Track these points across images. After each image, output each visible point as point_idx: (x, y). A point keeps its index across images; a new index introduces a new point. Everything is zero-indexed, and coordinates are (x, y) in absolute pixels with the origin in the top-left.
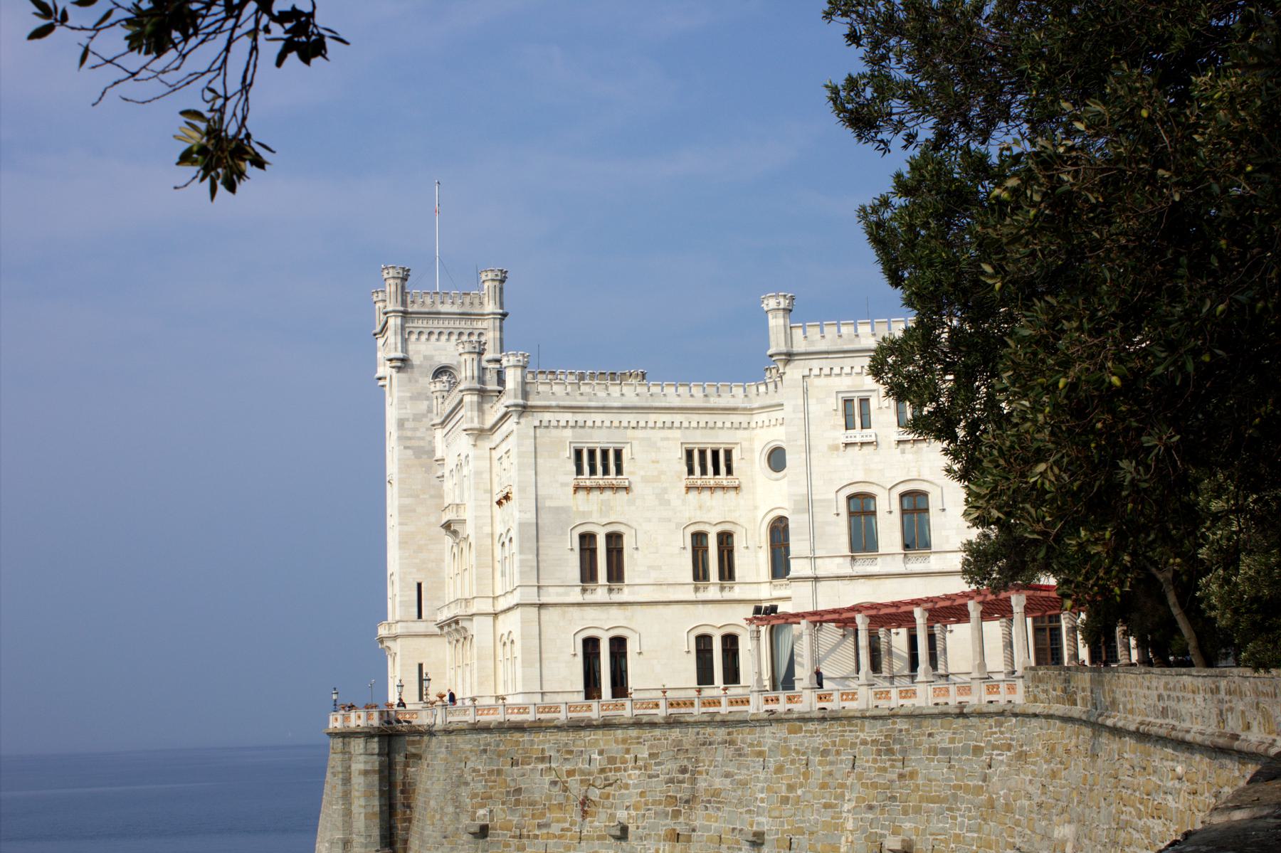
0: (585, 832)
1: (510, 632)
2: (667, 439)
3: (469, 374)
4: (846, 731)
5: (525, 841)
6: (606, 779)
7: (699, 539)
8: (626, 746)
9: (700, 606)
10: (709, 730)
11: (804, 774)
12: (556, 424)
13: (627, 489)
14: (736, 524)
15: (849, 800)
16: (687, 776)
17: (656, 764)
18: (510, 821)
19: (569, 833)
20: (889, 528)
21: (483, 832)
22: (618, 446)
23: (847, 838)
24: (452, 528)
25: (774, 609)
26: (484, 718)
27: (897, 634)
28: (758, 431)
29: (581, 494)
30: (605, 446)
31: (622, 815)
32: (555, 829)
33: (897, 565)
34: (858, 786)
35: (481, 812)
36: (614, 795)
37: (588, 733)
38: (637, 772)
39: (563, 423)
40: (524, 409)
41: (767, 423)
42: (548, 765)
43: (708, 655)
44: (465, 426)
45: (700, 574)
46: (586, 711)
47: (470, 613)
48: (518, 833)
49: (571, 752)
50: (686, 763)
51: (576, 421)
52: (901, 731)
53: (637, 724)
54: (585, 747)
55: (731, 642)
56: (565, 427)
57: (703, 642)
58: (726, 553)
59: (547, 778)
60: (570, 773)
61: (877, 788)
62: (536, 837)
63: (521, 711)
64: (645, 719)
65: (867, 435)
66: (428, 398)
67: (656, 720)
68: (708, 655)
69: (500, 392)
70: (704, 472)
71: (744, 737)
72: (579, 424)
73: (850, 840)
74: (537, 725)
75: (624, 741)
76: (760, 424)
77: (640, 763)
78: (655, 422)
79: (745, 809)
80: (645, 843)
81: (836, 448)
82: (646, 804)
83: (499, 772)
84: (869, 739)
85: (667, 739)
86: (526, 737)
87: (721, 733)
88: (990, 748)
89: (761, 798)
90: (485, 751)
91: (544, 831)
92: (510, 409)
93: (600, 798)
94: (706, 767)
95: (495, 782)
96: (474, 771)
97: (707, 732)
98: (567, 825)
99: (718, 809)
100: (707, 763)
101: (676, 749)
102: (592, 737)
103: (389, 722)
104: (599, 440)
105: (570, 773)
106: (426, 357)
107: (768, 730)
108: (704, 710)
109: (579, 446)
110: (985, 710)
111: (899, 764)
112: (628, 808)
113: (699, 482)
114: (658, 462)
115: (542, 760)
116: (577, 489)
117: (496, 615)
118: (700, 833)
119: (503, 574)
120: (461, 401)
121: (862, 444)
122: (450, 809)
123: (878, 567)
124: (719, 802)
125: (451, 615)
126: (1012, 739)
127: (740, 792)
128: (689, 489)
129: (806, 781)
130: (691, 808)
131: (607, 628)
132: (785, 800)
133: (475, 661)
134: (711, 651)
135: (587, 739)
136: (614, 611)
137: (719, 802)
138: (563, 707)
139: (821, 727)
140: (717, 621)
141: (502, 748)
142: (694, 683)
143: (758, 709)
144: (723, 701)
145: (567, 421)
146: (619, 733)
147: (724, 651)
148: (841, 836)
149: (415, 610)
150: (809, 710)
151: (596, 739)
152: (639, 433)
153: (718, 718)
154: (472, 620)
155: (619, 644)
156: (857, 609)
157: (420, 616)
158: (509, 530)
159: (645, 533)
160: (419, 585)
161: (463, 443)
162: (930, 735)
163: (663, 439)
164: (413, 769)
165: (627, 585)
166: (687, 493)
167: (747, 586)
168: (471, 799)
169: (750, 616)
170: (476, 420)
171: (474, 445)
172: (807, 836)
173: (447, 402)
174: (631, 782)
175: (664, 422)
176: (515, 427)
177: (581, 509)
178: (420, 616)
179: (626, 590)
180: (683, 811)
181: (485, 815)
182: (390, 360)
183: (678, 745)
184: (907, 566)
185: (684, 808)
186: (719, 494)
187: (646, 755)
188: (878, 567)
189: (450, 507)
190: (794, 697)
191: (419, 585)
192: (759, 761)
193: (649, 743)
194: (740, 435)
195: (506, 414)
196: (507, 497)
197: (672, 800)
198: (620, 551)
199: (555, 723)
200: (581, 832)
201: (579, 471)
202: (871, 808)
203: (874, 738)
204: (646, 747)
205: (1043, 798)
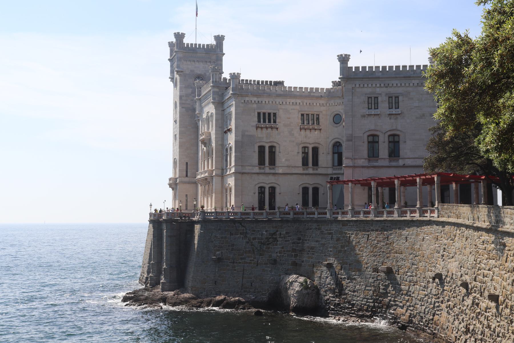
0: (259, 262)
2: (294, 109)
4: (365, 226)
5: (235, 264)
8: (277, 229)
12: (250, 102)
13: (277, 129)
14: (320, 144)
16: (301, 241)
17: (289, 236)
19: (253, 262)
20: (384, 150)
21: (219, 260)
22: (275, 112)
25: (338, 178)
27: (385, 189)
30: (270, 111)
31: (274, 255)
33: (386, 163)
35: (218, 253)
36: (271, 248)
41: (333, 104)
45: (305, 163)
48: (232, 261)
49: (254, 231)
51: (258, 101)
52: (387, 226)
55: (316, 190)
57: (305, 190)
58: (315, 155)
60: (254, 239)
62: (240, 263)
63: (235, 214)
64: (285, 219)
65: (378, 111)
66: (191, 88)
67: (289, 219)
80: (283, 266)
81: (363, 116)
84: (375, 229)
85: (293, 227)
87: (315, 225)
88: (423, 234)
89: (330, 250)
93: (266, 249)
95: (224, 241)
96: (215, 237)
97: (309, 225)
98: (252, 259)
99: (313, 254)
100: (309, 236)
101: (296, 231)
102: (263, 225)
105: (254, 239)
106: (191, 71)
109: (259, 111)
113: (306, 127)
114: (290, 118)
121: (375, 115)
123: (380, 163)
124: (313, 251)
125: (203, 176)
127: (321, 248)
128: (301, 129)
129: (349, 244)
130: (302, 254)
131: (267, 183)
132: (340, 251)
133: (214, 195)
134: (308, 193)
135: (261, 226)
137: (313, 251)
139: (356, 224)
140: (310, 181)
144: (316, 213)
147: (313, 193)
149: (185, 173)
153: (314, 219)
154: (213, 178)
155: (273, 190)
157: (187, 176)
159: (284, 146)
160: (187, 163)
163: (292, 109)
164: (189, 236)
166: (300, 131)
168: (214, 248)
172: (348, 265)
175: (293, 103)
177: (259, 136)
178: (187, 176)
179: (277, 168)
180: (299, 254)
181: (219, 254)
184: (390, 163)
185: (299, 253)
187: (284, 233)
188: (380, 163)
190: (345, 212)
191: (187, 163)
192: (330, 236)
193: (286, 228)
194: (322, 108)
195: (230, 97)
197: (294, 250)
198: (274, 153)
200: (258, 261)
201: (259, 121)
203: (377, 229)
205: (444, 253)
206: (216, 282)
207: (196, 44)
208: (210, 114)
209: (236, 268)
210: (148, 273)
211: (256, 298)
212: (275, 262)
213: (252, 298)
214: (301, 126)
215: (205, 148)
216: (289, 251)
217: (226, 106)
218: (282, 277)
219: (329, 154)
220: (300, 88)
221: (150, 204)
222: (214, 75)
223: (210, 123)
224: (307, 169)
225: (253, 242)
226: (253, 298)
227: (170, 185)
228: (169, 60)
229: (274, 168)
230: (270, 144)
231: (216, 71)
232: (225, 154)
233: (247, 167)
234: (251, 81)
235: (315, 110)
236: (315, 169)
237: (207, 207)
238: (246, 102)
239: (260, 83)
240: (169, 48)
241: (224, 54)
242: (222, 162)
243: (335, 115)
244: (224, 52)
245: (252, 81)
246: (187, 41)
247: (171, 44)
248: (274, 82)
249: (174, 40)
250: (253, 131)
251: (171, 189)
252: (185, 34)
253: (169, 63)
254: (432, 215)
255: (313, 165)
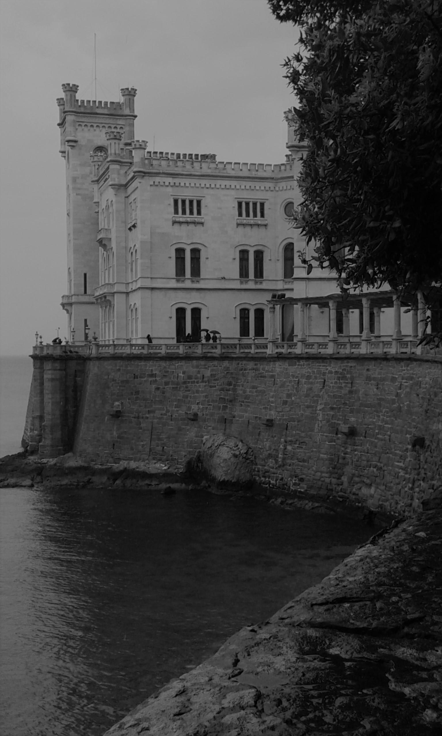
0: (174, 416)
1: (135, 304)
3: (113, 152)
4: (320, 366)
5: (141, 420)
6: (187, 387)
7: (244, 254)
9: (243, 292)
10: (244, 362)
11: (296, 388)
12: (162, 184)
13: (202, 224)
15: (320, 404)
18: (133, 409)
19: (165, 417)
21: (117, 415)
23: (318, 425)
24: (103, 243)
25: (283, 296)
26: (119, 351)
27: (353, 312)
28: (280, 193)
29: (177, 226)
31: (195, 408)
32: (158, 414)
34: (326, 396)
35: (117, 403)
37: (177, 362)
38: (204, 384)
39: (167, 184)
40: (144, 174)
41: (285, 188)
42: (154, 379)
43: (246, 320)
44: (111, 183)
45: (244, 273)
46: (176, 349)
47: (113, 292)
49: (167, 372)
50: (231, 379)
51: (175, 183)
52: (351, 367)
53: (205, 358)
54: (175, 369)
55: (260, 313)
56: (167, 186)
57: (244, 313)
59: (154, 386)
60: (167, 383)
61: (336, 398)
62: (147, 418)
64: (209, 355)
67: (215, 355)
68: (246, 320)
69: (131, 163)
70: (248, 215)
71: (265, 368)
72: (176, 185)
73: (320, 426)
74: (148, 356)
75: (197, 367)
76: (281, 188)
77: (206, 379)
78: (220, 185)
79: (263, 407)
82: (208, 402)
83: (127, 382)
84: (334, 371)
86: (143, 363)
87: (251, 365)
90: (119, 370)
91: (152, 415)
92: (136, 174)
93: (183, 397)
94: (242, 383)
98: (164, 412)
99: (248, 406)
100: (243, 380)
101: (226, 372)
103: (65, 352)
104: (188, 194)
105: (167, 383)
107: (277, 364)
108: (242, 351)
110: (399, 357)
111: (350, 385)
112: (198, 404)
114: (220, 208)
115: (152, 375)
116: (174, 222)
117: (127, 294)
118: (237, 419)
119: (132, 270)
120: (108, 168)
122: (99, 401)
124: (249, 402)
125: (101, 293)
126: (413, 374)
127: (260, 397)
128: (238, 225)
132: (285, 403)
135: (177, 365)
136: (194, 294)
137: (249, 402)
138: (164, 347)
139: (307, 363)
141: (129, 368)
142: (239, 336)
143: (272, 352)
145: (169, 183)
146: (194, 362)
147: (256, 318)
148: (316, 423)
149: (83, 289)
150: (300, 353)
151: (182, 365)
152: (211, 191)
153: (250, 356)
154: (114, 296)
155: (196, 312)
156: (330, 297)
158: (135, 245)
160: (85, 275)
161: (110, 194)
162: (368, 370)
165: (202, 279)
167: (270, 282)
169: (270, 299)
170: (116, 179)
171: (115, 195)
173: (100, 168)
174: (200, 389)
176: (139, 185)
180: (229, 406)
181: (119, 405)
182: (68, 141)
183: (227, 369)
186: (255, 229)
189: (102, 231)
191: (85, 275)
196: (134, 226)
197: (222, 400)
199: (159, 355)
200: (172, 416)
201: (176, 212)
202: (332, 409)
204: (209, 370)
205: (429, 407)
206: (114, 445)
207: (94, 102)
208: (110, 202)
209: (142, 425)
210: (32, 430)
211: (169, 468)
212: (195, 418)
213: (163, 468)
214: (238, 220)
215: (105, 253)
216: (216, 401)
217: (130, 189)
218: (205, 437)
219: (278, 260)
220: (235, 163)
221: (35, 333)
222: (113, 144)
223: (111, 215)
224: (247, 282)
225: (164, 388)
226: (165, 468)
227: (63, 305)
228: (59, 125)
229: (198, 281)
230: (193, 246)
231: (116, 139)
232: (130, 261)
233: (158, 280)
234: (167, 153)
235: (258, 196)
236: (259, 283)
237: (109, 337)
238: (156, 184)
239: (181, 157)
240: (58, 108)
241: (136, 116)
242: (126, 272)
243: (287, 205)
244: (136, 113)
245: (170, 154)
246: (80, 96)
247: (61, 102)
248: (201, 155)
249: (62, 95)
250: (167, 227)
251: (65, 312)
252: (78, 86)
253: (58, 130)
254: (413, 350)
255: (256, 276)
